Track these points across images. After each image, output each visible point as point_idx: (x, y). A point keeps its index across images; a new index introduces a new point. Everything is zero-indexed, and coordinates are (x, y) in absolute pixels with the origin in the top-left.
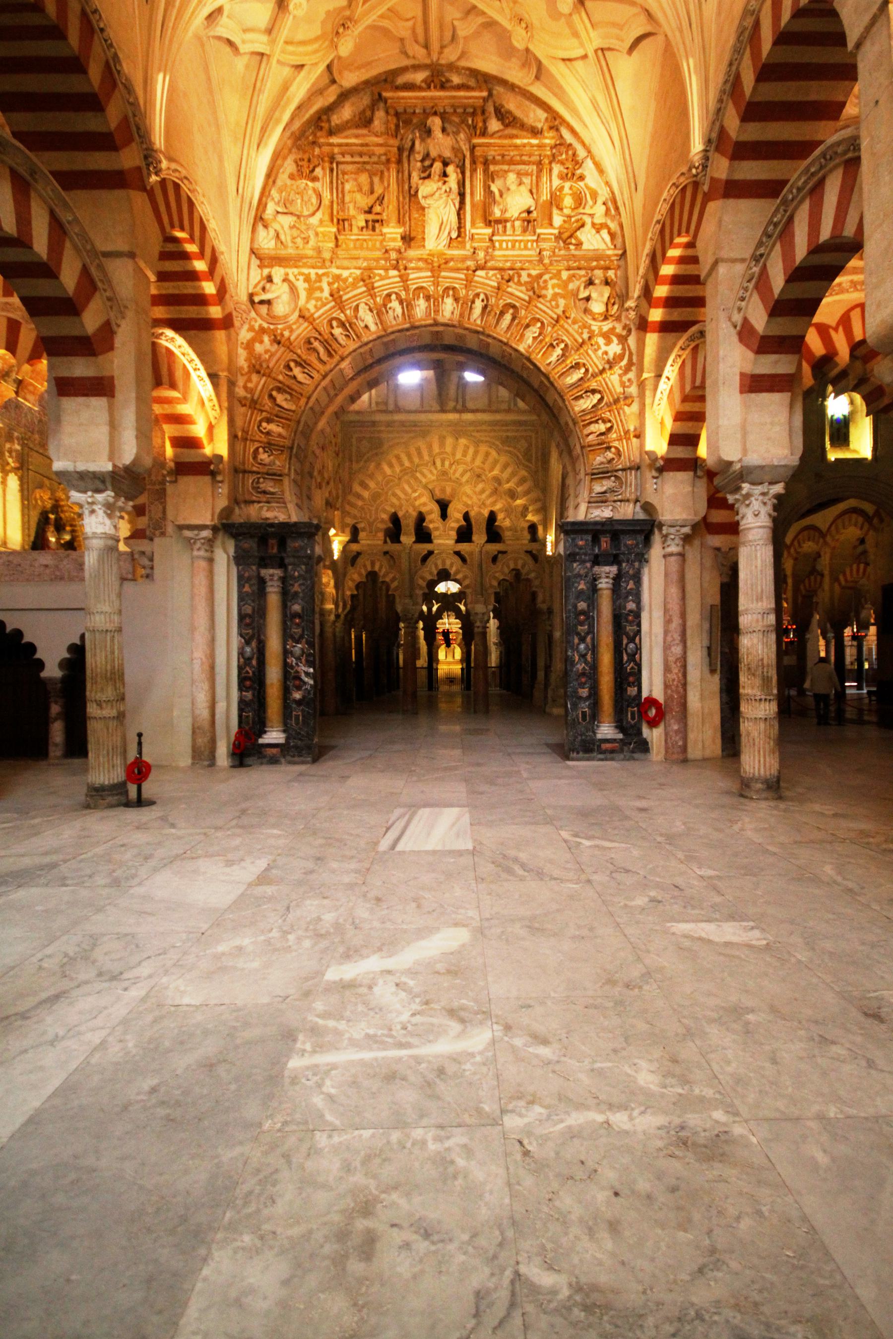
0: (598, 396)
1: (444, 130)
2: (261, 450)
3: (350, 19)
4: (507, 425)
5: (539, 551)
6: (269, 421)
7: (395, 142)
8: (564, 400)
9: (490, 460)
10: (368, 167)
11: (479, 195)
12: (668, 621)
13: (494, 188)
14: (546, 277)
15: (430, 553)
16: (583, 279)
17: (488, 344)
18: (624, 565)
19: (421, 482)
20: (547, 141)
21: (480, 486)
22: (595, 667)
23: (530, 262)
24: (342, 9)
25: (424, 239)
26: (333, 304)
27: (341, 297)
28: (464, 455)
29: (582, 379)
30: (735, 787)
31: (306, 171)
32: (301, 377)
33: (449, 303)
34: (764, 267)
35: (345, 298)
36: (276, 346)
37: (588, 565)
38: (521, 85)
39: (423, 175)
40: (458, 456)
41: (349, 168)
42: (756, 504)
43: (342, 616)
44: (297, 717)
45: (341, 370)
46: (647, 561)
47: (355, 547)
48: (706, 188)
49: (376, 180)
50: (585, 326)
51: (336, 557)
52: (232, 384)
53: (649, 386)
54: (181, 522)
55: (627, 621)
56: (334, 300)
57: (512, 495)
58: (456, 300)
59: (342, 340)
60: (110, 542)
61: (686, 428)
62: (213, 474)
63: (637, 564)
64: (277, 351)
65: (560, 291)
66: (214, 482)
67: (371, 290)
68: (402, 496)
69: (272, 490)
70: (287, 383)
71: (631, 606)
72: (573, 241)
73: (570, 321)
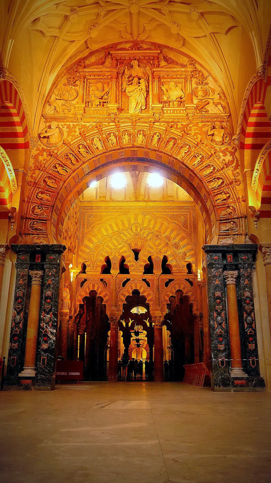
0: (222, 181)
1: (139, 66)
4: (173, 209)
6: (42, 193)
8: (202, 183)
9: (164, 227)
10: (102, 81)
14: (191, 125)
15: (128, 280)
18: (241, 270)
20: (189, 69)
21: (158, 242)
22: (227, 332)
26: (81, 137)
27: (85, 134)
32: (61, 172)
33: (140, 138)
35: (87, 135)
37: (221, 270)
38: (176, 48)
43: (74, 317)
47: (83, 276)
49: (106, 86)
51: (72, 281)
52: (25, 175)
57: (177, 246)
59: (84, 154)
62: (10, 218)
64: (50, 159)
65: (198, 132)
67: (100, 132)
68: (113, 247)
69: (40, 228)
71: (248, 294)
72: (204, 110)
73: (204, 145)
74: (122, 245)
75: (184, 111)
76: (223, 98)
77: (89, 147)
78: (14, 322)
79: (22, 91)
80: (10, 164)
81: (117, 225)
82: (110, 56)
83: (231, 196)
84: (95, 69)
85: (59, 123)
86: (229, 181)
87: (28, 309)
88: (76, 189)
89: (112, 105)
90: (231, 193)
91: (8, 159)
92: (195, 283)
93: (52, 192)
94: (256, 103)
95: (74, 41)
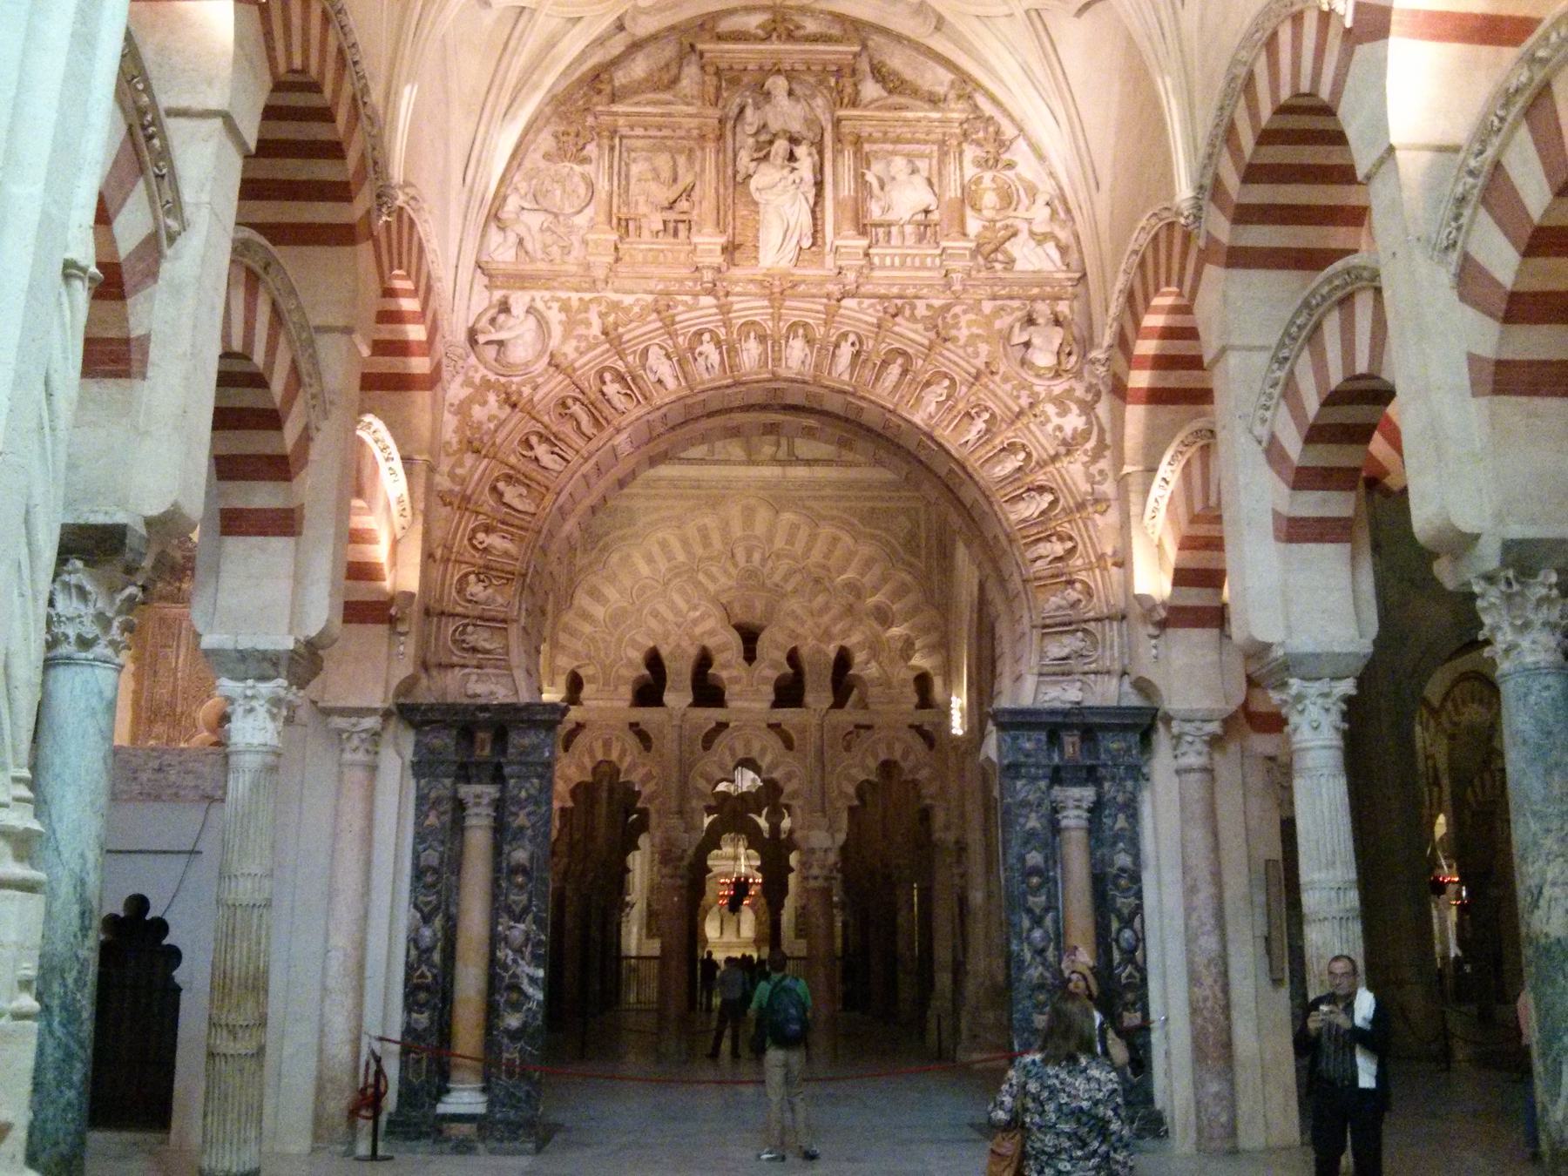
0: (1049, 497)
1: (790, 93)
2: (472, 578)
5: (939, 724)
6: (488, 530)
7: (715, 113)
8: (991, 504)
10: (669, 143)
11: (847, 188)
12: (1190, 891)
13: (870, 177)
14: (957, 309)
15: (722, 726)
16: (1019, 314)
17: (862, 409)
18: (1107, 785)
19: (706, 590)
20: (955, 115)
21: (820, 600)
27: (620, 336)
28: (790, 540)
29: (1020, 468)
31: (570, 149)
32: (547, 460)
34: (1292, 372)
35: (625, 338)
36: (508, 409)
37: (1043, 784)
38: (912, 36)
39: (756, 155)
40: (779, 543)
41: (639, 143)
45: (614, 448)
52: (432, 469)
53: (1135, 485)
55: (1117, 886)
56: (610, 342)
58: (809, 341)
59: (620, 402)
62: (392, 621)
63: (1129, 784)
65: (980, 331)
66: (394, 632)
67: (669, 326)
68: (670, 616)
69: (488, 646)
70: (523, 469)
71: (1123, 860)
73: (997, 378)
74: (702, 609)
75: (937, 261)
76: (1062, 215)
77: (633, 379)
78: (417, 948)
79: (427, 216)
80: (396, 455)
81: (685, 543)
82: (694, 58)
83: (1080, 547)
85: (537, 294)
86: (1074, 497)
88: (587, 502)
89: (707, 240)
90: (1078, 539)
91: (389, 441)
93: (521, 528)
94: (1168, 284)
95: (580, 19)
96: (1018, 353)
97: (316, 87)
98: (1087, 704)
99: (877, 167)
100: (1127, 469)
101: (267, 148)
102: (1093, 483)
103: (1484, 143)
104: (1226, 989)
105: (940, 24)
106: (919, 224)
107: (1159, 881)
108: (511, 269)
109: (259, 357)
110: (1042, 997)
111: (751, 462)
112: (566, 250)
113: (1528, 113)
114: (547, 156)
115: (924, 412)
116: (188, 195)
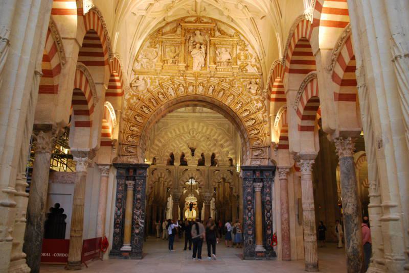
1: (200, 34)
3: (172, 7)
6: (133, 126)
9: (213, 132)
12: (282, 205)
13: (217, 52)
14: (235, 80)
18: (265, 182)
21: (209, 143)
23: (229, 75)
24: (170, 4)
25: (192, 66)
28: (202, 130)
30: (304, 267)
31: (153, 45)
32: (146, 111)
36: (138, 101)
37: (252, 182)
40: (200, 130)
41: (167, 44)
42: (305, 167)
44: (136, 240)
45: (161, 109)
46: (273, 181)
47: (153, 167)
48: (284, 68)
49: (177, 48)
50: (249, 97)
52: (121, 113)
53: (272, 118)
54: (99, 163)
58: (203, 87)
59: (162, 99)
60: (84, 174)
61: (284, 135)
62: (112, 146)
63: (270, 182)
67: (173, 83)
68: (175, 146)
71: (268, 198)
79: (121, 59)
80: (113, 110)
82: (180, 26)
84: (169, 37)
85: (145, 76)
87: (125, 206)
88: (156, 120)
92: (234, 174)
96: (248, 90)
97: (96, 33)
98: (262, 165)
99: (219, 50)
100: (270, 115)
101: (84, 45)
102: (264, 118)
103: (337, 49)
104: (289, 226)
105: (232, 20)
106: (227, 62)
107: (275, 203)
108: (140, 71)
109: (83, 90)
110: (250, 227)
111: (194, 112)
112: (152, 67)
113: (346, 42)
114: (148, 47)
115: (228, 102)
116: (67, 55)
